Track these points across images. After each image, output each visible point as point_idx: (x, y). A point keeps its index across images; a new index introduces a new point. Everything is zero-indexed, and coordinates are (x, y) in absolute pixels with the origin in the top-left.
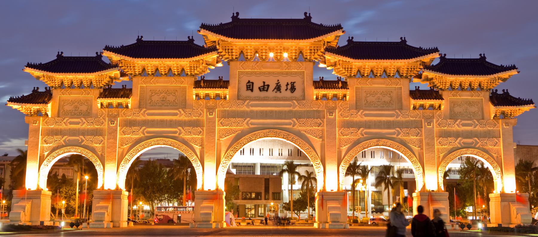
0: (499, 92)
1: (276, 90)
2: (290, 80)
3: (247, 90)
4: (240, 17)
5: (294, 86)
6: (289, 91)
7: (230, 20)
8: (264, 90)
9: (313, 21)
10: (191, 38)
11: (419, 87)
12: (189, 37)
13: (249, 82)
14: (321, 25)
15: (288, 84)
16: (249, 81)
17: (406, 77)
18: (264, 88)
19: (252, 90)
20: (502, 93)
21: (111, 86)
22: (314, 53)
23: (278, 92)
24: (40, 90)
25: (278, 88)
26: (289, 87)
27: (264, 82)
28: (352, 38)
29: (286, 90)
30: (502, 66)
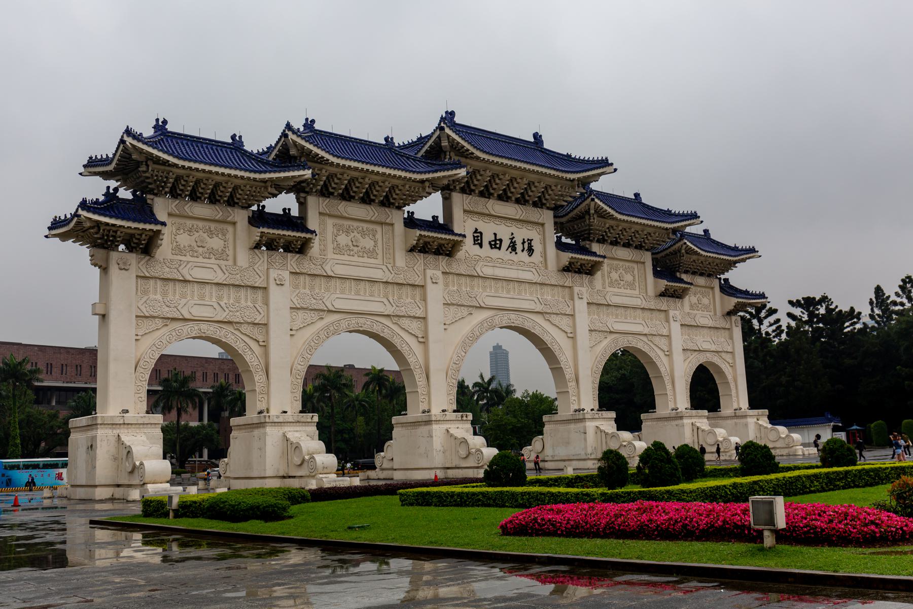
4: (457, 120)
6: (525, 252)
8: (496, 248)
9: (546, 146)
13: (476, 231)
14: (569, 156)
15: (524, 243)
16: (476, 229)
17: (647, 250)
18: (496, 244)
19: (481, 245)
21: (264, 207)
25: (513, 247)
26: (526, 245)
27: (495, 234)
29: (523, 251)
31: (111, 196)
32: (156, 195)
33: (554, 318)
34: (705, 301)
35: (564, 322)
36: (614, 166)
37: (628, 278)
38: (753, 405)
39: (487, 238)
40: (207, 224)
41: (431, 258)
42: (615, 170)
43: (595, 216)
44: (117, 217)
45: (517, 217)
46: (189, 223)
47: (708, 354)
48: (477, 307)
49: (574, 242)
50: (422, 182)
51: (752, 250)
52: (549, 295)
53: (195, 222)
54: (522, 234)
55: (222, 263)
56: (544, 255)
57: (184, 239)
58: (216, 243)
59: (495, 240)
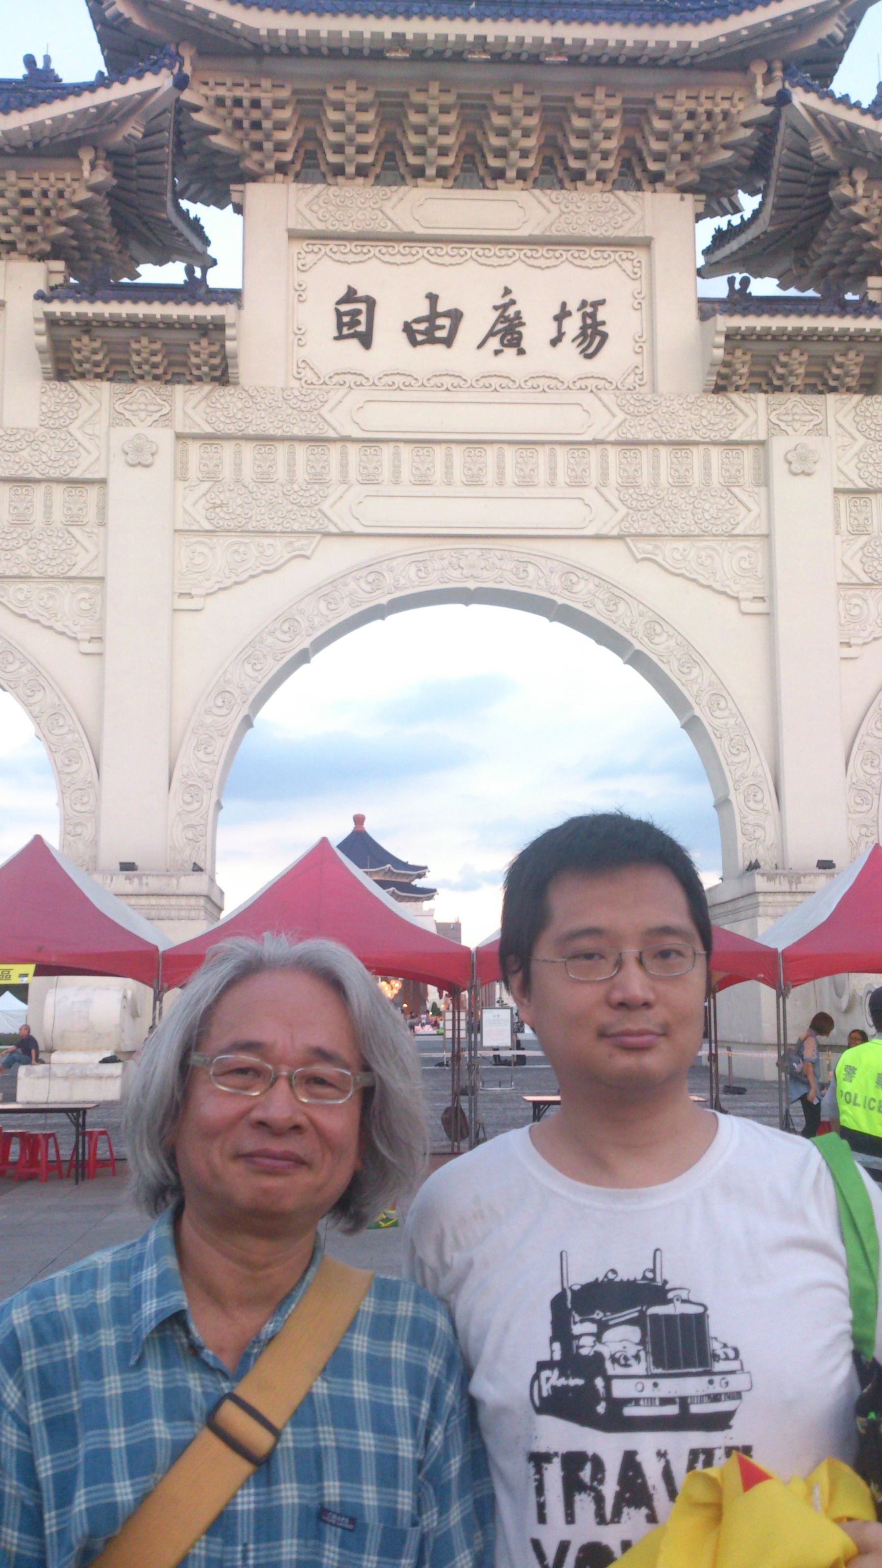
1: (494, 343)
3: (340, 337)
5: (596, 324)
6: (569, 348)
8: (432, 340)
13: (350, 296)
15: (563, 314)
18: (433, 328)
19: (366, 340)
23: (511, 352)
25: (509, 332)
26: (572, 326)
27: (433, 299)
29: (554, 342)
33: (670, 552)
41: (144, 394)
43: (860, 176)
45: (525, 232)
48: (327, 535)
49: (811, 293)
56: (646, 344)
59: (434, 315)
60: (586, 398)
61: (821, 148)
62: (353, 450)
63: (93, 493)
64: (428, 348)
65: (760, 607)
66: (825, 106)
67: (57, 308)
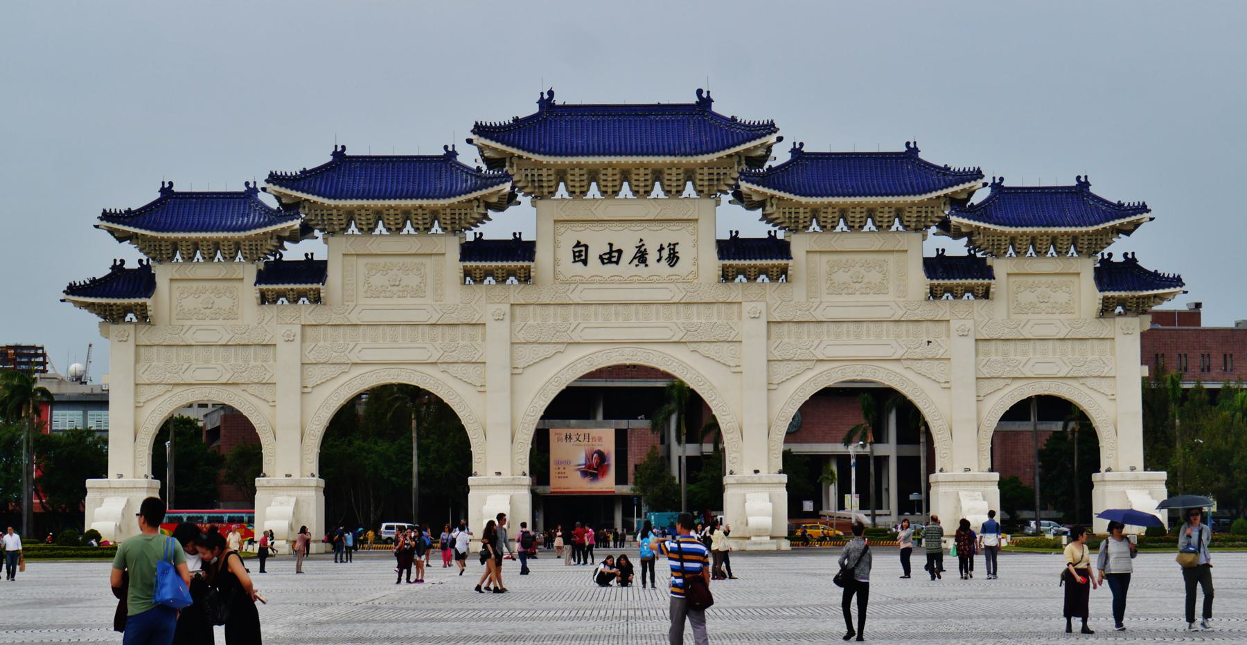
0: (1114, 259)
1: (636, 262)
2: (666, 236)
4: (558, 100)
6: (664, 263)
7: (535, 109)
8: (610, 262)
10: (450, 149)
11: (943, 250)
12: (446, 147)
13: (578, 244)
15: (662, 248)
18: (612, 256)
19: (585, 262)
20: (1122, 260)
21: (281, 255)
22: (718, 180)
23: (642, 265)
24: (126, 266)
25: (641, 257)
26: (665, 253)
27: (611, 245)
28: (802, 145)
29: (659, 261)
30: (1120, 205)
31: (118, 268)
32: (160, 261)
33: (703, 348)
34: (1061, 297)
35: (725, 351)
36: (778, 134)
37: (874, 277)
38: (1150, 465)
39: (597, 249)
40: (214, 284)
42: (780, 139)
44: (102, 296)
46: (195, 285)
47: (1045, 383)
50: (470, 201)
51: (1143, 208)
52: (698, 317)
53: (201, 284)
54: (654, 239)
55: (231, 322)
56: (696, 261)
57: (190, 303)
58: (225, 302)
59: (611, 251)
60: (671, 286)
61: (755, 198)
62: (579, 308)
63: (479, 330)
64: (609, 266)
65: (738, 369)
66: (755, 187)
67: (468, 264)
